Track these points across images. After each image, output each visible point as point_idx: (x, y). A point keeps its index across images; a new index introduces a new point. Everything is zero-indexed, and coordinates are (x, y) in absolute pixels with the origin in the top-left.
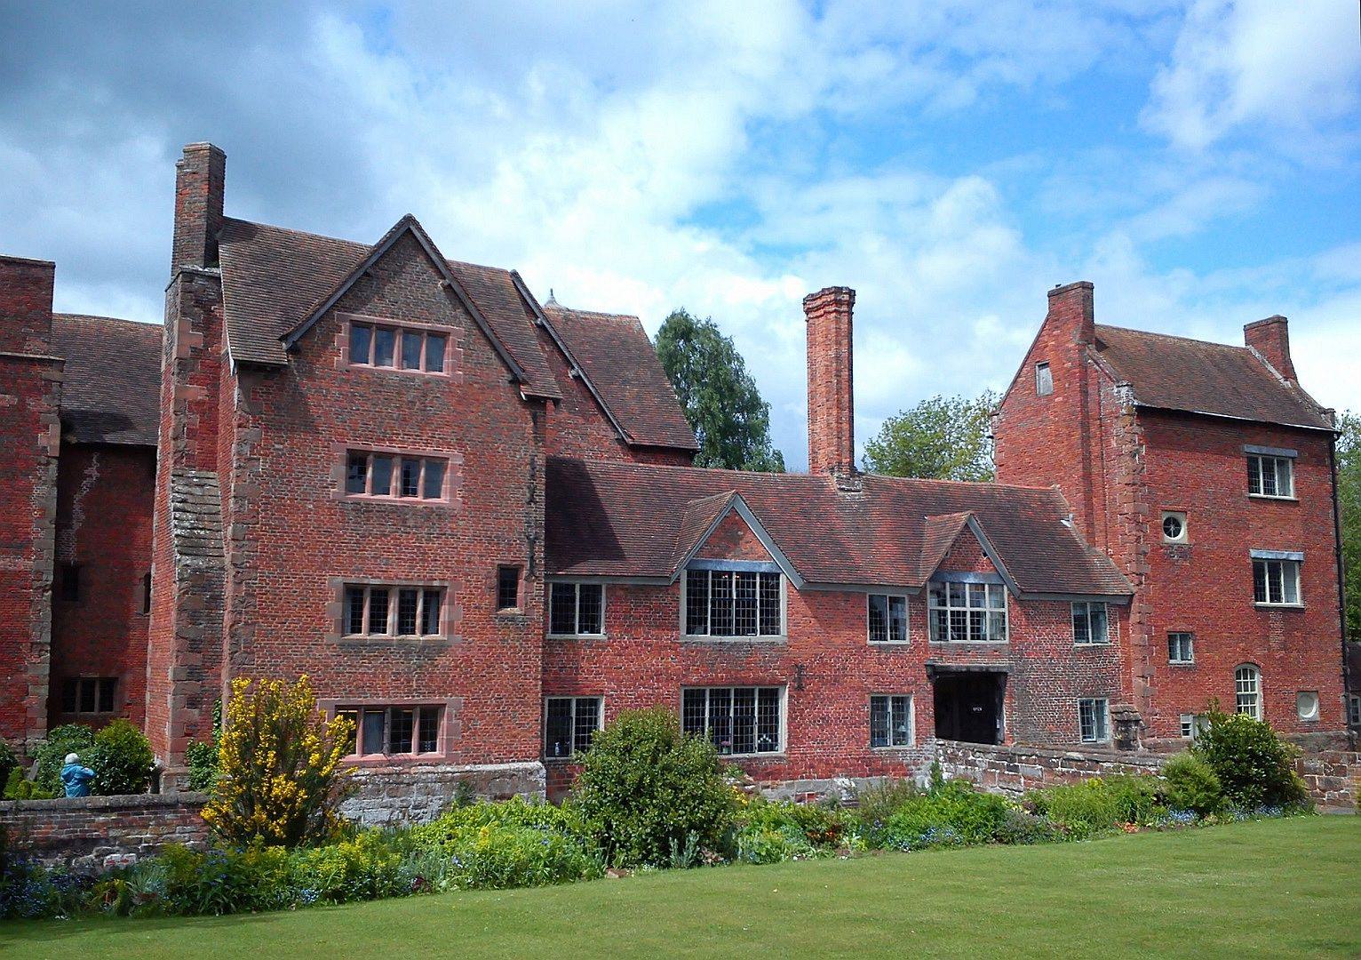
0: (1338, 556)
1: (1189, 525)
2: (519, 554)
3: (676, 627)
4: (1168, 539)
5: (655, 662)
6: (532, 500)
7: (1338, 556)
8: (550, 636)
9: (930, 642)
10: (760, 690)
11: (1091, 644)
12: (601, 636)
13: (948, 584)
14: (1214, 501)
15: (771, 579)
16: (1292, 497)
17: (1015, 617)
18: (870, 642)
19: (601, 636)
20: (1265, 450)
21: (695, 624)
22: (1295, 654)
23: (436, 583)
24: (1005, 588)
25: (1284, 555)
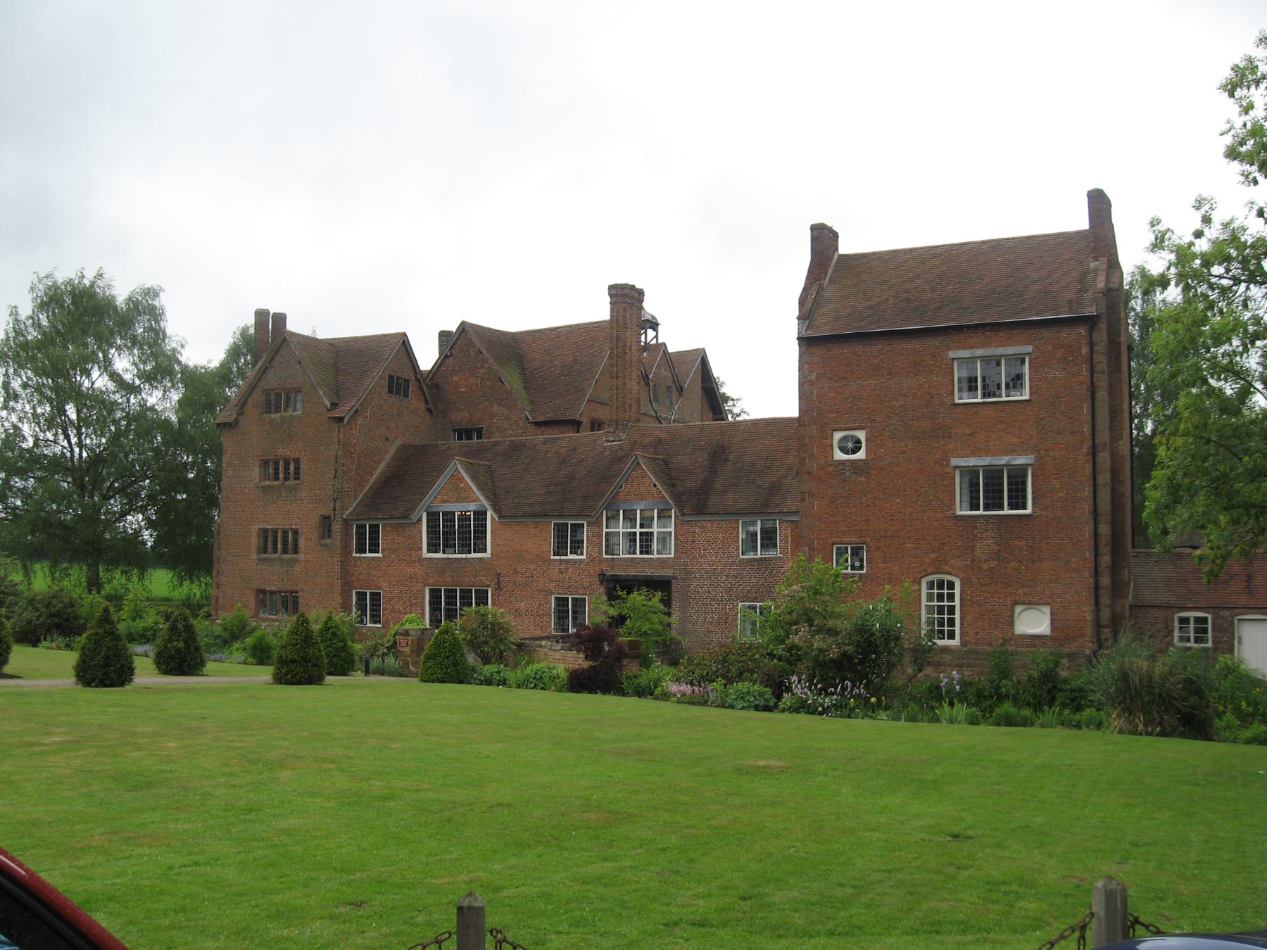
0: (1094, 455)
1: (867, 440)
2: (326, 510)
3: (421, 549)
4: (839, 456)
5: (409, 571)
6: (335, 477)
7: (1094, 455)
8: (355, 555)
9: (604, 556)
10: (475, 590)
11: (759, 556)
12: (380, 555)
13: (621, 511)
14: (903, 414)
15: (480, 515)
16: (1026, 397)
17: (682, 535)
18: (552, 557)
19: (380, 555)
20: (979, 352)
21: (433, 547)
22: (1013, 564)
23: (294, 527)
24: (673, 510)
25: (1003, 460)
